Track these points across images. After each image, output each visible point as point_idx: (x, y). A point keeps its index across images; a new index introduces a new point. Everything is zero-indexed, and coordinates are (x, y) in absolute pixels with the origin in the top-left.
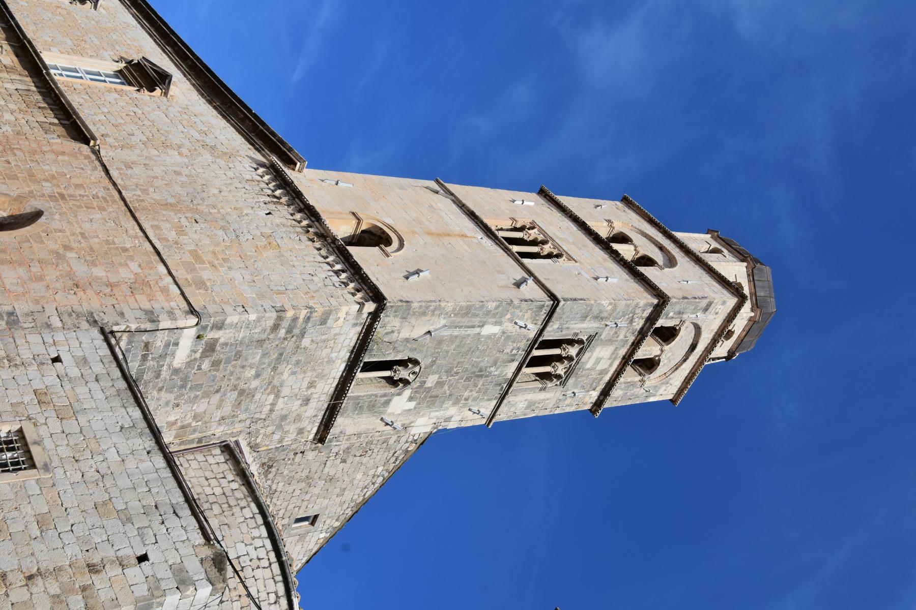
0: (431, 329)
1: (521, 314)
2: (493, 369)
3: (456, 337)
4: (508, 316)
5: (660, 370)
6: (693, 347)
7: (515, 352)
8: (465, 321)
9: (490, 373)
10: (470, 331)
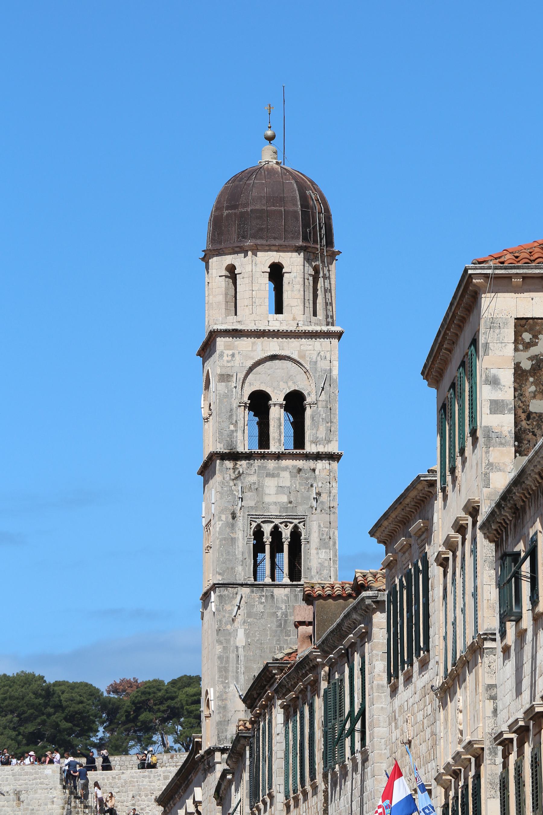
0: (237, 695)
1: (227, 615)
2: (279, 614)
3: (246, 667)
4: (229, 627)
5: (302, 384)
6: (273, 357)
7: (263, 600)
8: (232, 666)
9: (283, 613)
10: (242, 658)
